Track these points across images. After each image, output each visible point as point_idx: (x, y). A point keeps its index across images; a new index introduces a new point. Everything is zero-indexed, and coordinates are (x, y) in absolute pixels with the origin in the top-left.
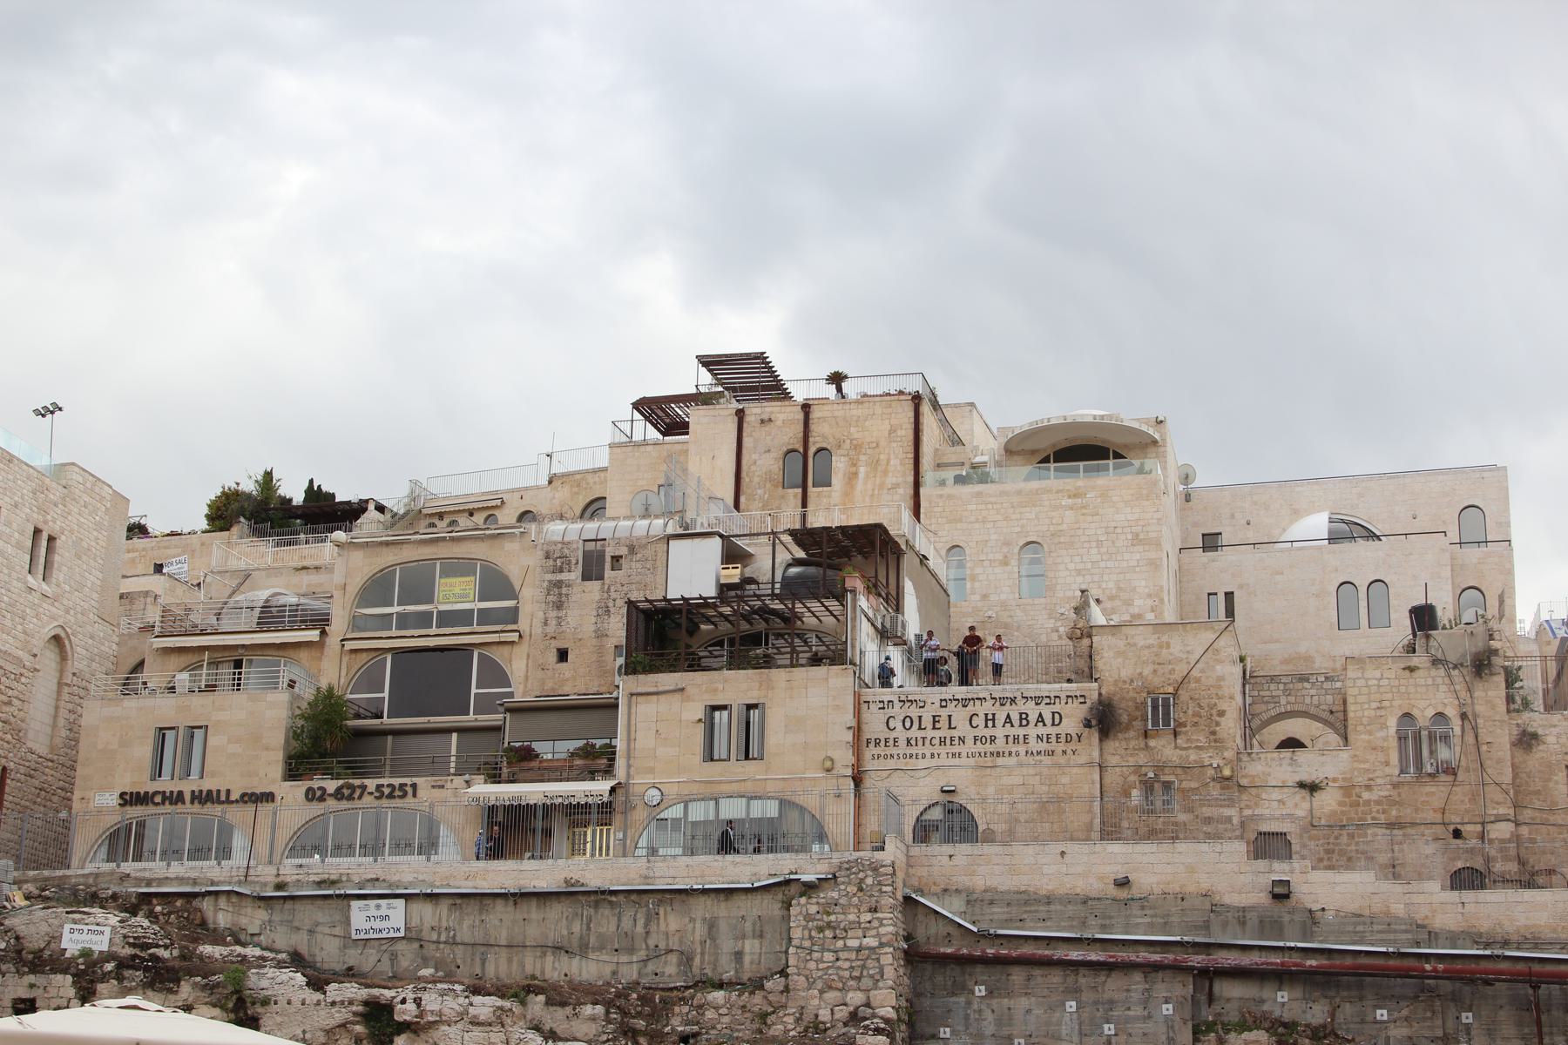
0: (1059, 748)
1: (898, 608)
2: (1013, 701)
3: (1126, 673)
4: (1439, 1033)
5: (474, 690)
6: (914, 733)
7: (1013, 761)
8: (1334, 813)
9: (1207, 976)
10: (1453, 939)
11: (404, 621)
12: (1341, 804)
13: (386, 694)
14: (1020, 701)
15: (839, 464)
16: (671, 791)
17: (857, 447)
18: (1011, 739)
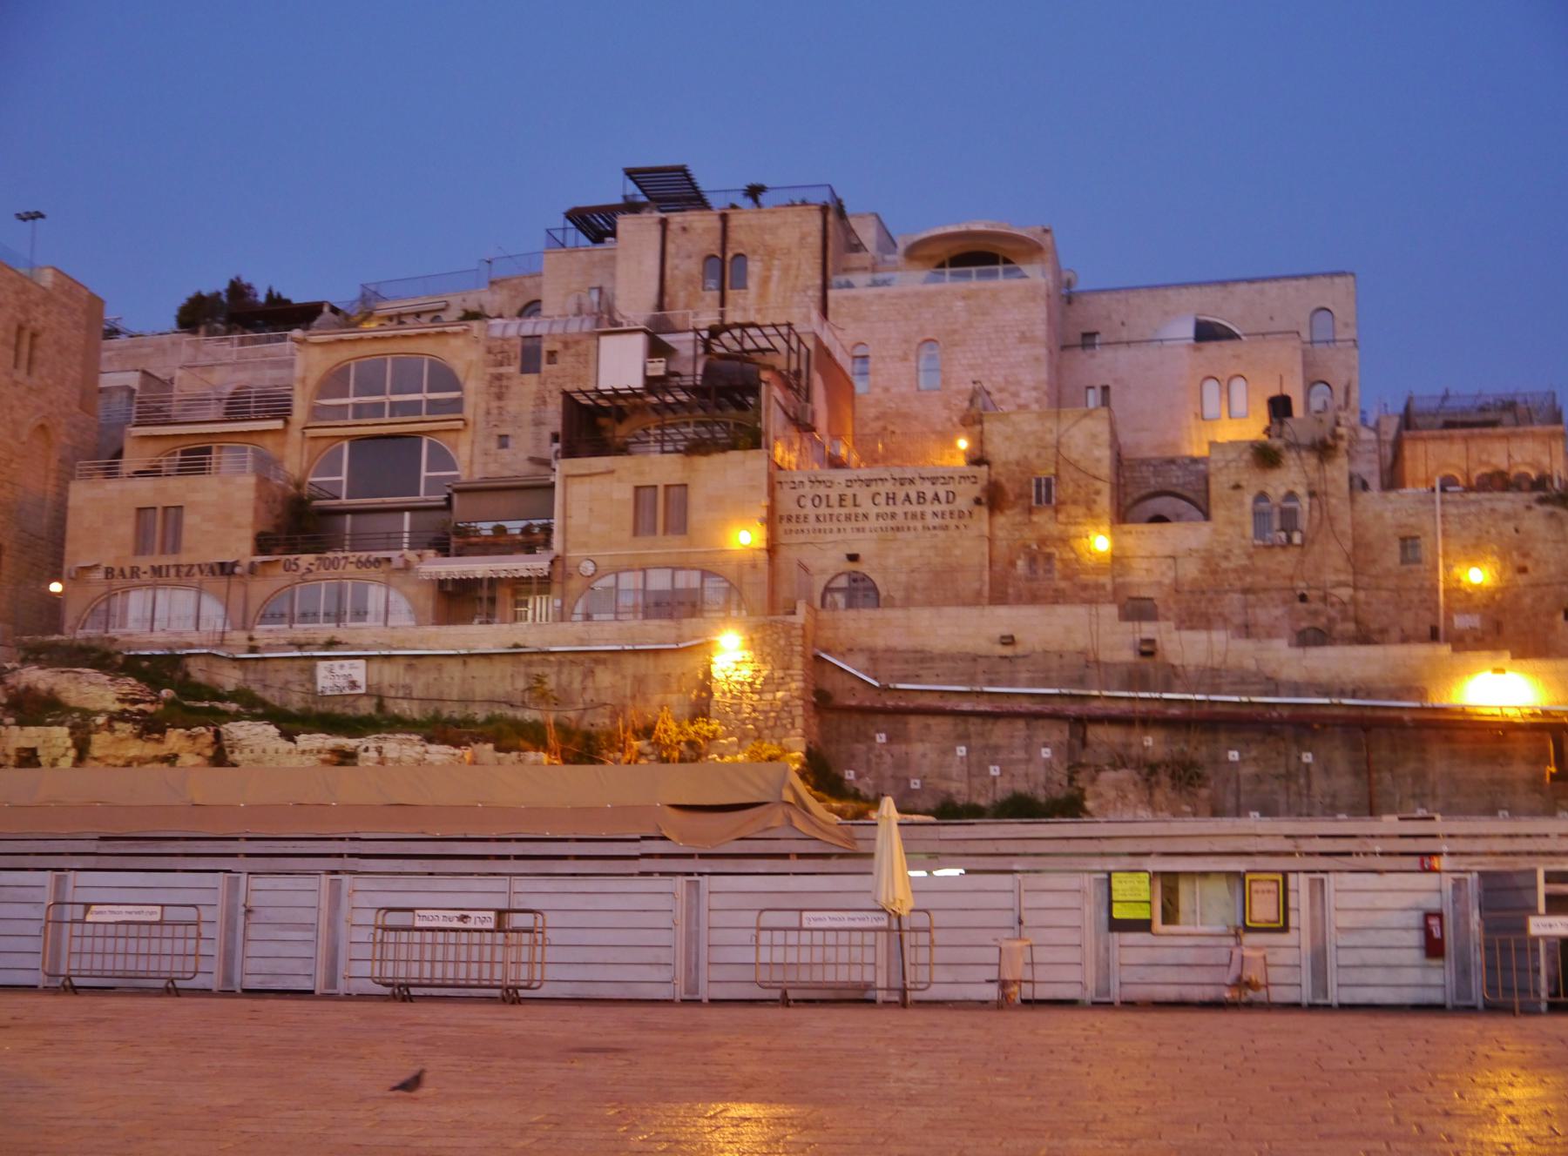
0: (952, 523)
1: (808, 399)
2: (912, 481)
3: (1014, 455)
4: (1282, 771)
5: (424, 473)
6: (823, 510)
7: (909, 536)
8: (1195, 580)
9: (1081, 723)
10: (1297, 689)
11: (359, 410)
12: (1202, 572)
13: (344, 478)
14: (918, 481)
15: (754, 267)
16: (603, 563)
17: (771, 253)
18: (909, 516)
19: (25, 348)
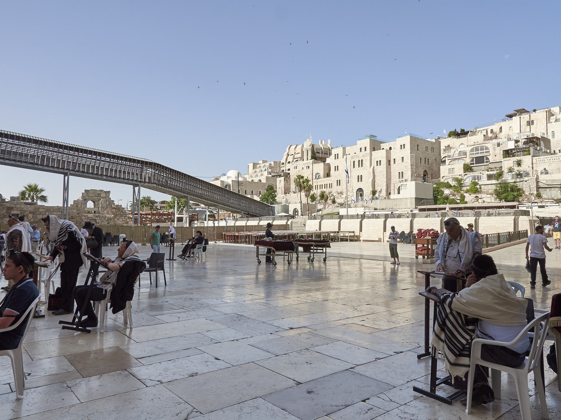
5: (485, 161)
6: (540, 162)
11: (476, 154)
13: (474, 162)
15: (535, 122)
17: (538, 119)
19: (433, 150)
